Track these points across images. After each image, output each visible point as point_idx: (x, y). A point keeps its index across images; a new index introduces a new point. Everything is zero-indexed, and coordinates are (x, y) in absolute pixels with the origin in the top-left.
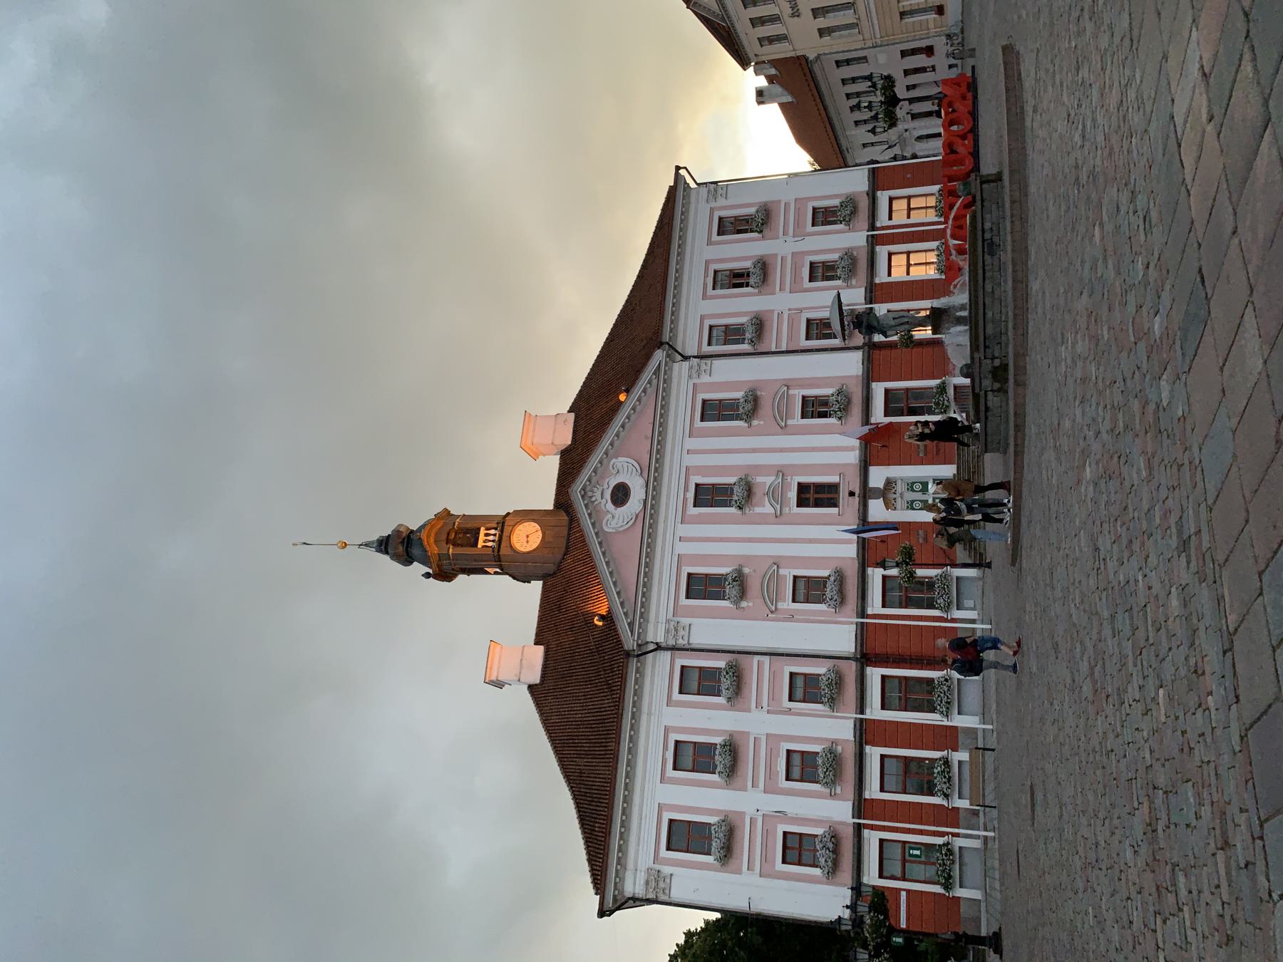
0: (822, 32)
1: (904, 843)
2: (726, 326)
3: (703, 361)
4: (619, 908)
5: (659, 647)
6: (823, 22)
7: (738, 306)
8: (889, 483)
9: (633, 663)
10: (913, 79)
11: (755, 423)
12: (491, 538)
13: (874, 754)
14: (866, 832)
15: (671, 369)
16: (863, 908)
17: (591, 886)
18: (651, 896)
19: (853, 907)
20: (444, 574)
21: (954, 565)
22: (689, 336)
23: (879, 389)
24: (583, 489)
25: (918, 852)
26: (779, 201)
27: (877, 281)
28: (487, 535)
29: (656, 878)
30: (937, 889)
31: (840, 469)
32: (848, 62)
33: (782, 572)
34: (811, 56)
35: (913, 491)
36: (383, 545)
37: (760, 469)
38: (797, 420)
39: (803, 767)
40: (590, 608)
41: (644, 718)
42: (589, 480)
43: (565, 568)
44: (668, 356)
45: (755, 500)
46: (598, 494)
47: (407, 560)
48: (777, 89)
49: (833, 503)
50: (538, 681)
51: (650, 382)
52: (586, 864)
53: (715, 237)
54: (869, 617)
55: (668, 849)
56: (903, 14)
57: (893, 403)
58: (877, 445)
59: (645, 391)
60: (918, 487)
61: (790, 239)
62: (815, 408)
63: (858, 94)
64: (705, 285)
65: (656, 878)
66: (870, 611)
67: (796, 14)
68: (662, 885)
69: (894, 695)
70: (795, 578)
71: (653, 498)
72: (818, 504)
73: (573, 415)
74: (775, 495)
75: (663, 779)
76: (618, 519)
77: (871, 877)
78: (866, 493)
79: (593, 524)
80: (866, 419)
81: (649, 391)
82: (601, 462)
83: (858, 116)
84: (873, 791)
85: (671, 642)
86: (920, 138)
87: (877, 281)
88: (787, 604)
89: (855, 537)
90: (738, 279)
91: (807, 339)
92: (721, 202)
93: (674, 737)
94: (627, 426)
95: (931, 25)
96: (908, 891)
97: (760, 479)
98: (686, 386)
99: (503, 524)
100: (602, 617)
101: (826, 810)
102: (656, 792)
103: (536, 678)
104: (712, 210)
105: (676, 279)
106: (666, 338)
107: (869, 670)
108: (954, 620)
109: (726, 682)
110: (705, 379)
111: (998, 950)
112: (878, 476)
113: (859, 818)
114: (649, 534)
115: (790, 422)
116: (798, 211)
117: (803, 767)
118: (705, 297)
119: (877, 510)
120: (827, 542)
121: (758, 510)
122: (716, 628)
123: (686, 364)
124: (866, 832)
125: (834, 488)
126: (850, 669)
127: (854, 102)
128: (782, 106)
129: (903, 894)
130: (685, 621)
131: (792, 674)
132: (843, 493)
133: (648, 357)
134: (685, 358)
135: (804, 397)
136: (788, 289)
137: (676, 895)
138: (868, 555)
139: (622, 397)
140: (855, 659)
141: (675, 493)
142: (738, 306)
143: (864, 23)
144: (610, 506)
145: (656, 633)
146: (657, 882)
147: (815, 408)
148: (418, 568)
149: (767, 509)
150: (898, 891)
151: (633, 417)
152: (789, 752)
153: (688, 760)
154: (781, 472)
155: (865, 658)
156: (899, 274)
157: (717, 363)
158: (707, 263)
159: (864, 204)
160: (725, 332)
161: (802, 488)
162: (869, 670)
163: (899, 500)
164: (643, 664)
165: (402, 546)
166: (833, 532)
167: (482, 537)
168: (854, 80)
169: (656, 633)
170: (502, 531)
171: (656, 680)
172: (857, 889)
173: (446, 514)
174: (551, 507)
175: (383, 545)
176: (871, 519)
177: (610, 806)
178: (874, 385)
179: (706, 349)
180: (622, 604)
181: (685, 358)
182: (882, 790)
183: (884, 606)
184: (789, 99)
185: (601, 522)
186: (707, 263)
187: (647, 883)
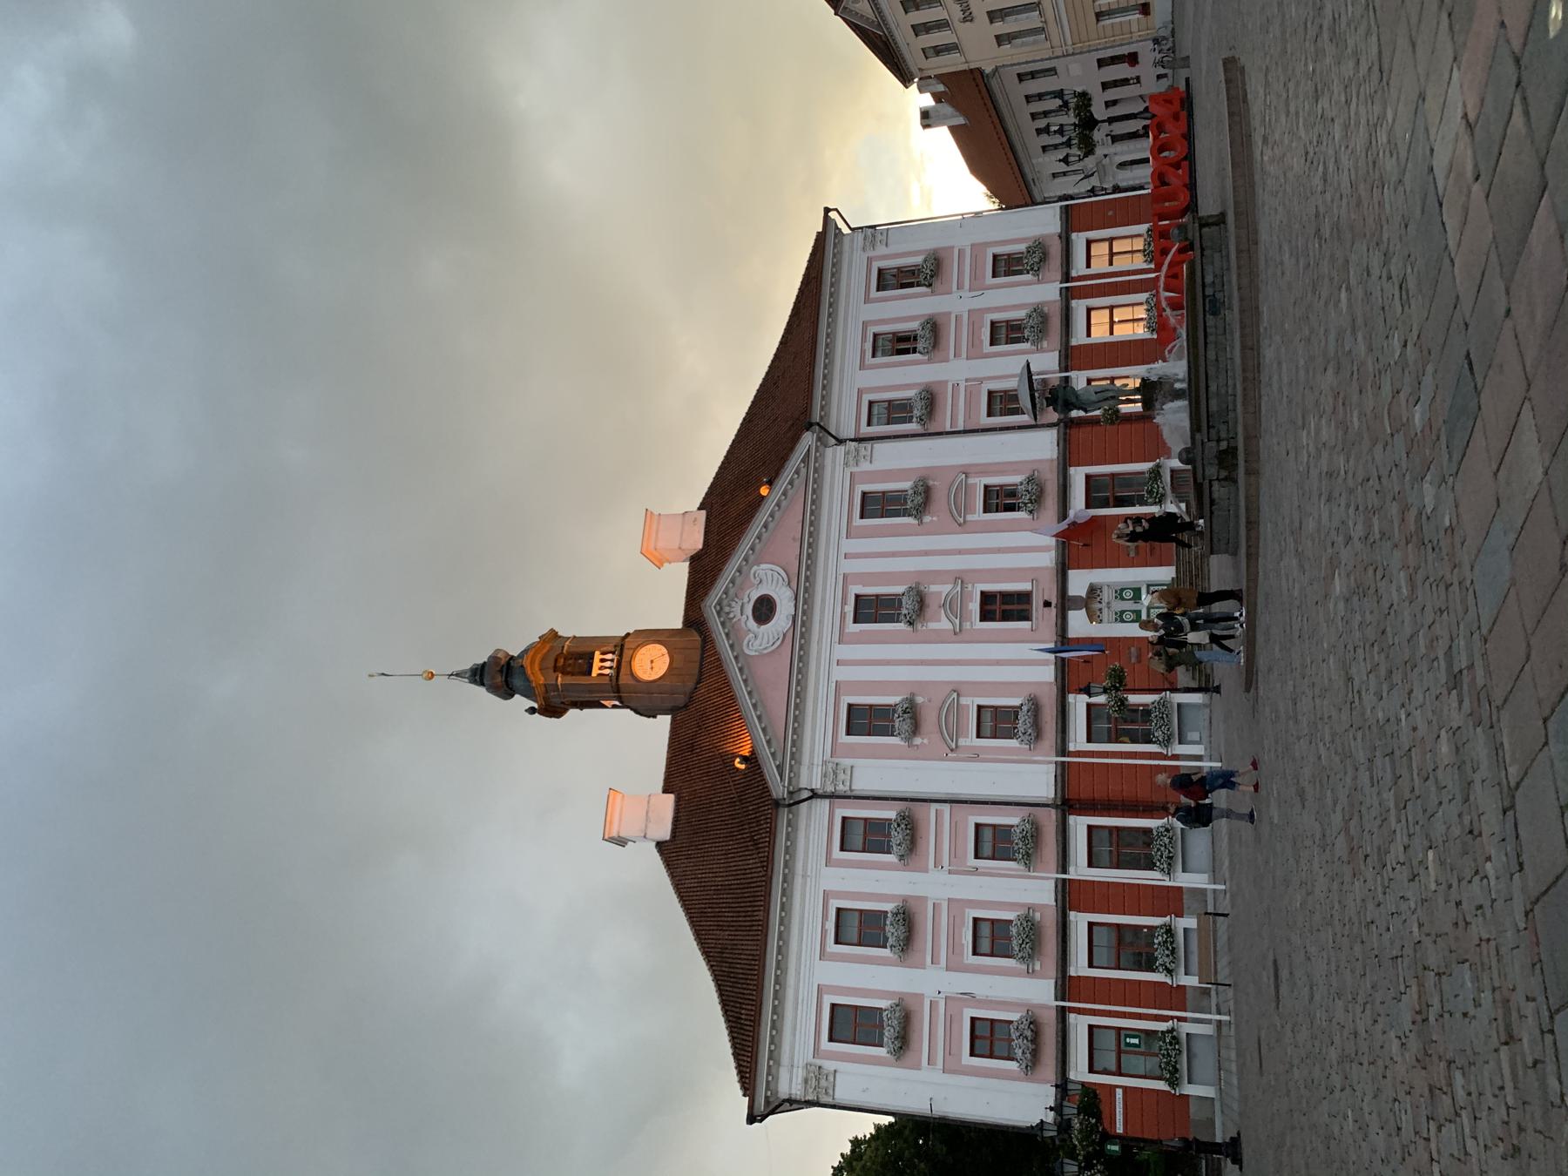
0: (1000, 40)
1: (1119, 1029)
2: (889, 401)
3: (862, 445)
4: (773, 1112)
5: (814, 795)
6: (1001, 27)
7: (903, 377)
8: (1093, 590)
9: (784, 815)
10: (1113, 94)
11: (927, 519)
12: (608, 664)
13: (1079, 921)
14: (1072, 1017)
15: (822, 455)
16: (1070, 1110)
17: (738, 1086)
18: (810, 1097)
19: (1057, 1109)
20: (552, 708)
21: (1174, 690)
22: (845, 414)
23: (1078, 475)
24: (719, 603)
25: (1136, 1041)
26: (952, 248)
27: (1074, 342)
28: (603, 660)
29: (816, 1075)
30: (1161, 1085)
31: (1033, 574)
32: (1033, 75)
33: (963, 701)
34: (988, 70)
35: (1123, 599)
36: (478, 675)
37: (937, 576)
38: (978, 515)
39: (993, 938)
40: (729, 748)
41: (798, 881)
42: (726, 592)
43: (699, 702)
44: (819, 439)
45: (929, 612)
46: (737, 609)
47: (506, 690)
48: (947, 109)
49: (1025, 616)
50: (668, 838)
51: (797, 472)
52: (731, 1058)
53: (874, 294)
54: (1070, 754)
55: (831, 1039)
56: (1099, 16)
57: (1097, 492)
58: (1078, 545)
59: (791, 483)
60: (1129, 594)
61: (966, 294)
62: (1000, 500)
63: (1046, 114)
64: (863, 352)
65: (816, 1075)
66: (1072, 747)
67: (968, 18)
68: (823, 1083)
69: (1104, 849)
70: (980, 708)
71: (804, 613)
72: (1006, 617)
73: (704, 513)
74: (953, 607)
75: (823, 955)
76: (761, 639)
77: (1079, 1072)
78: (1065, 603)
79: (732, 646)
80: (1063, 515)
81: (796, 482)
82: (739, 571)
83: (1046, 140)
84: (1079, 966)
85: (830, 789)
86: (1122, 165)
87: (1074, 342)
88: (970, 740)
89: (1052, 657)
90: (902, 344)
91: (989, 415)
92: (881, 250)
93: (835, 904)
94: (771, 526)
95: (1134, 28)
96: (1125, 1089)
97: (934, 588)
98: (841, 476)
99: (621, 647)
100: (745, 759)
101: (1022, 990)
102: (815, 972)
103: (665, 834)
104: (870, 260)
105: (824, 387)
106: (816, 417)
107: (1072, 819)
108: (1176, 757)
109: (892, 931)
110: (865, 466)
111: (1237, 1160)
112: (1079, 582)
113: (1063, 1000)
114: (800, 658)
115: (969, 517)
116: (972, 324)
117: (993, 938)
118: (862, 367)
119: (1079, 624)
120: (1019, 664)
121: (932, 625)
122: (884, 771)
123: (841, 449)
124: (1072, 1017)
125: (1025, 597)
126: (1049, 819)
127: (1042, 123)
128: (953, 130)
129: (1119, 1092)
131: (978, 826)
132: (1037, 602)
133: (795, 439)
135: (986, 487)
136: (964, 355)
137: (841, 1095)
138: (1068, 679)
139: (764, 491)
140: (1053, 805)
141: (831, 606)
142: (903, 377)
143: (1052, 28)
144: (752, 624)
145: (811, 777)
146: (818, 1080)
147: (1000, 500)
148: (521, 702)
149: (944, 624)
150: (1113, 1088)
151: (777, 515)
152: (975, 920)
153: (852, 932)
154: (960, 578)
155: (1067, 804)
156: (1100, 333)
157: (879, 447)
158: (865, 325)
159: (1056, 249)
160: (888, 408)
161: (986, 598)
162: (1072, 819)
163: (1105, 611)
164: (796, 815)
165: (500, 676)
166: (1026, 651)
167: (596, 664)
168: (1040, 96)
169: (811, 777)
170: (621, 655)
171: (814, 831)
172: (1063, 1086)
173: (553, 635)
174: (680, 626)
175: (478, 675)
176: (1072, 634)
177: (760, 988)
178: (1072, 470)
179: (865, 430)
180: (768, 742)
181: (840, 442)
182: (1091, 965)
183: (1089, 740)
184: (961, 120)
185: (741, 645)
186: (865, 325)
187: (806, 1081)
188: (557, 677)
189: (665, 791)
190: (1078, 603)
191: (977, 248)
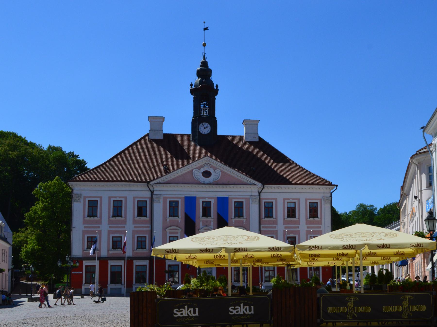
3: (258, 200)
5: (152, 192)
9: (146, 184)
12: (205, 112)
36: (204, 64)
47: (199, 74)
64: (289, 199)
73: (257, 140)
93: (123, 200)
96: (82, 274)
123: (257, 194)
129: (81, 273)
130: (161, 200)
131: (146, 237)
134: (260, 193)
144: (202, 170)
150: (82, 271)
158: (299, 200)
165: (204, 72)
175: (204, 64)
179: (263, 201)
181: (260, 193)
188: (205, 93)
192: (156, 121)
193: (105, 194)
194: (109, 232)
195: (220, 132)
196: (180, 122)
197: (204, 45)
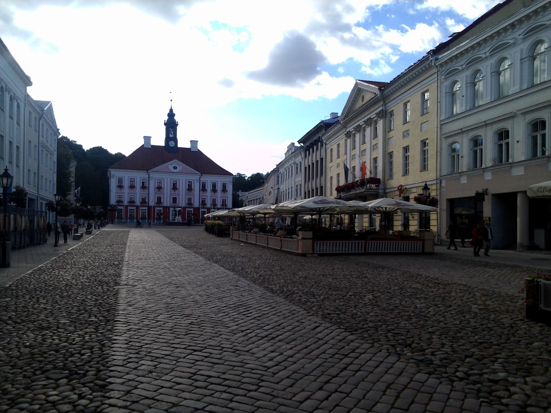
7: (209, 187)
13: (135, 208)
36: (171, 110)
37: (179, 192)
47: (169, 115)
76: (171, 168)
78: (174, 208)
119: (172, 209)
126: (147, 205)
138: (165, 208)
142: (209, 187)
154: (179, 194)
157: (198, 184)
175: (171, 110)
179: (201, 182)
188: (171, 125)
189: (152, 146)
190: (174, 209)
191: (227, 197)
192: (147, 139)
193: (126, 175)
194: (128, 193)
195: (179, 146)
196: (159, 140)
197: (171, 100)
